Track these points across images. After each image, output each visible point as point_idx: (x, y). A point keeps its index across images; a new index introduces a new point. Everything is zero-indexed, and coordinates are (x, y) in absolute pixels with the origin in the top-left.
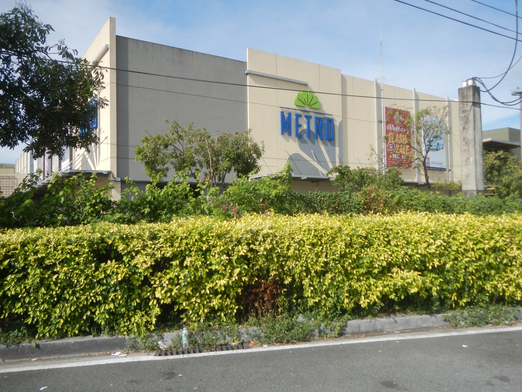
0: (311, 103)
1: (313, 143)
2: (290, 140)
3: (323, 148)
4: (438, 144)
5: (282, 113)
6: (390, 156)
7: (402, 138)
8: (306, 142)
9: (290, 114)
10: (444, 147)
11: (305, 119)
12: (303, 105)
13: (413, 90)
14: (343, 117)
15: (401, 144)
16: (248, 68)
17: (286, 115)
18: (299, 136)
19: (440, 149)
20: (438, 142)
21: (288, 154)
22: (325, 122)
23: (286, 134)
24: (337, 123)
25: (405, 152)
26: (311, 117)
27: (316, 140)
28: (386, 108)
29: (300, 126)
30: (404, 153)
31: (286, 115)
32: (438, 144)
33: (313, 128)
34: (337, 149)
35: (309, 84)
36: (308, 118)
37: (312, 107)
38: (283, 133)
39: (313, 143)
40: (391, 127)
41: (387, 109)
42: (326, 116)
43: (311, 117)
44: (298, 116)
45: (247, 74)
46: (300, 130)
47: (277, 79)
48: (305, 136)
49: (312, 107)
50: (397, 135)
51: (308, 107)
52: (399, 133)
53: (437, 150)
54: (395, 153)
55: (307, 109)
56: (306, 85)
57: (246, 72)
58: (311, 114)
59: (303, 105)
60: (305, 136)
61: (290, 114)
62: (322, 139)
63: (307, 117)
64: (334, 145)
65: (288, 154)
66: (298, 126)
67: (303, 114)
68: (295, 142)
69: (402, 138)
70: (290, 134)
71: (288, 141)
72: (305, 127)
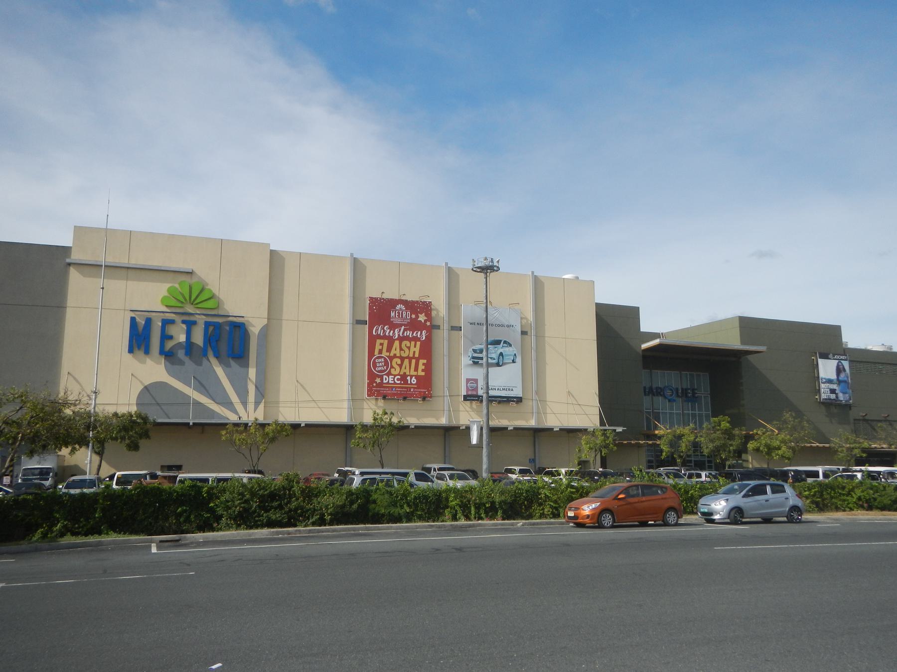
0: (196, 302)
1: (199, 364)
2: (149, 361)
3: (219, 371)
4: (501, 354)
5: (133, 320)
6: (378, 380)
7: (409, 348)
8: (181, 363)
9: (149, 321)
10: (519, 359)
11: (184, 326)
12: (180, 305)
13: (444, 264)
14: (268, 319)
15: (408, 357)
16: (75, 257)
17: (141, 322)
18: (169, 355)
19: (503, 364)
20: (501, 350)
21: (141, 382)
22: (227, 328)
23: (140, 354)
24: (255, 329)
25: (416, 369)
26: (195, 323)
27: (205, 361)
28: (371, 298)
29: (171, 338)
30: (413, 373)
31: (141, 322)
32: (501, 354)
33: (198, 338)
34: (252, 372)
35: (197, 271)
36: (190, 325)
37: (199, 306)
38: (131, 351)
39: (199, 364)
40: (378, 330)
41: (373, 300)
42: (231, 319)
43: (195, 323)
44: (166, 323)
45: (69, 264)
46: (169, 345)
47: (128, 268)
48: (181, 354)
49: (200, 306)
50: (397, 343)
51: (192, 306)
52: (401, 339)
53: (498, 365)
54: (389, 374)
55: (190, 309)
56: (190, 273)
57: (68, 261)
58: (197, 318)
59: (180, 305)
60: (181, 354)
61: (149, 321)
62: (217, 356)
63: (184, 322)
64: (246, 365)
65: (141, 382)
66: (165, 337)
67: (178, 319)
68: (161, 364)
69: (409, 348)
70: (147, 352)
71: (144, 363)
72: (182, 338)
